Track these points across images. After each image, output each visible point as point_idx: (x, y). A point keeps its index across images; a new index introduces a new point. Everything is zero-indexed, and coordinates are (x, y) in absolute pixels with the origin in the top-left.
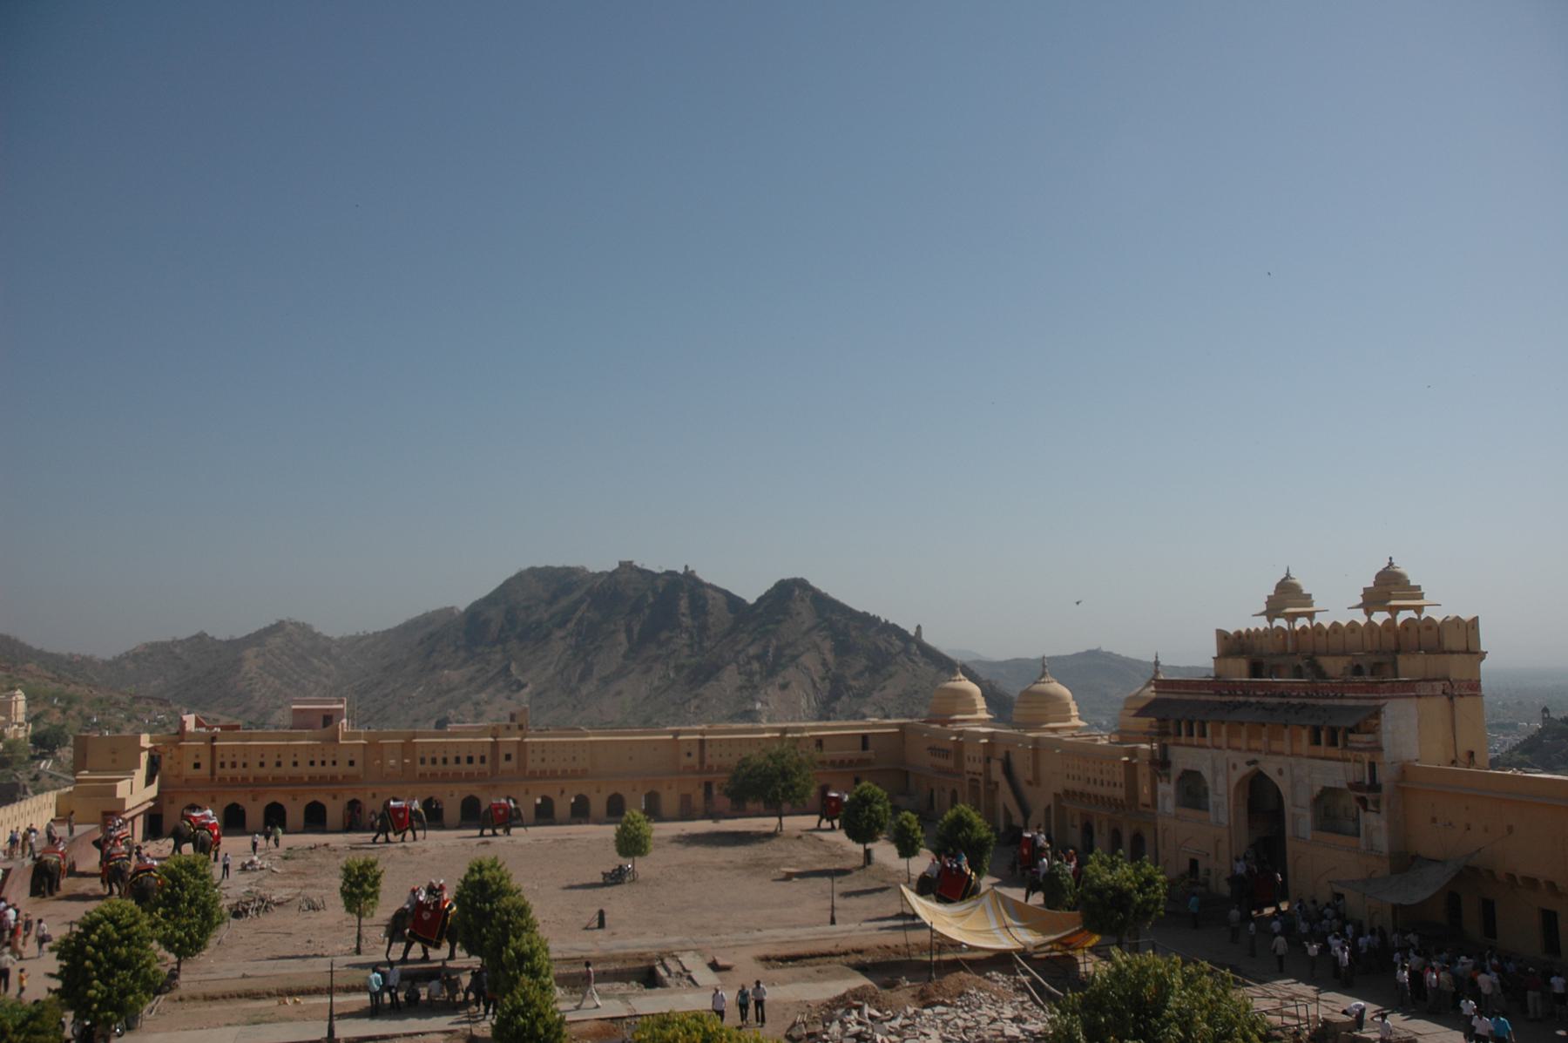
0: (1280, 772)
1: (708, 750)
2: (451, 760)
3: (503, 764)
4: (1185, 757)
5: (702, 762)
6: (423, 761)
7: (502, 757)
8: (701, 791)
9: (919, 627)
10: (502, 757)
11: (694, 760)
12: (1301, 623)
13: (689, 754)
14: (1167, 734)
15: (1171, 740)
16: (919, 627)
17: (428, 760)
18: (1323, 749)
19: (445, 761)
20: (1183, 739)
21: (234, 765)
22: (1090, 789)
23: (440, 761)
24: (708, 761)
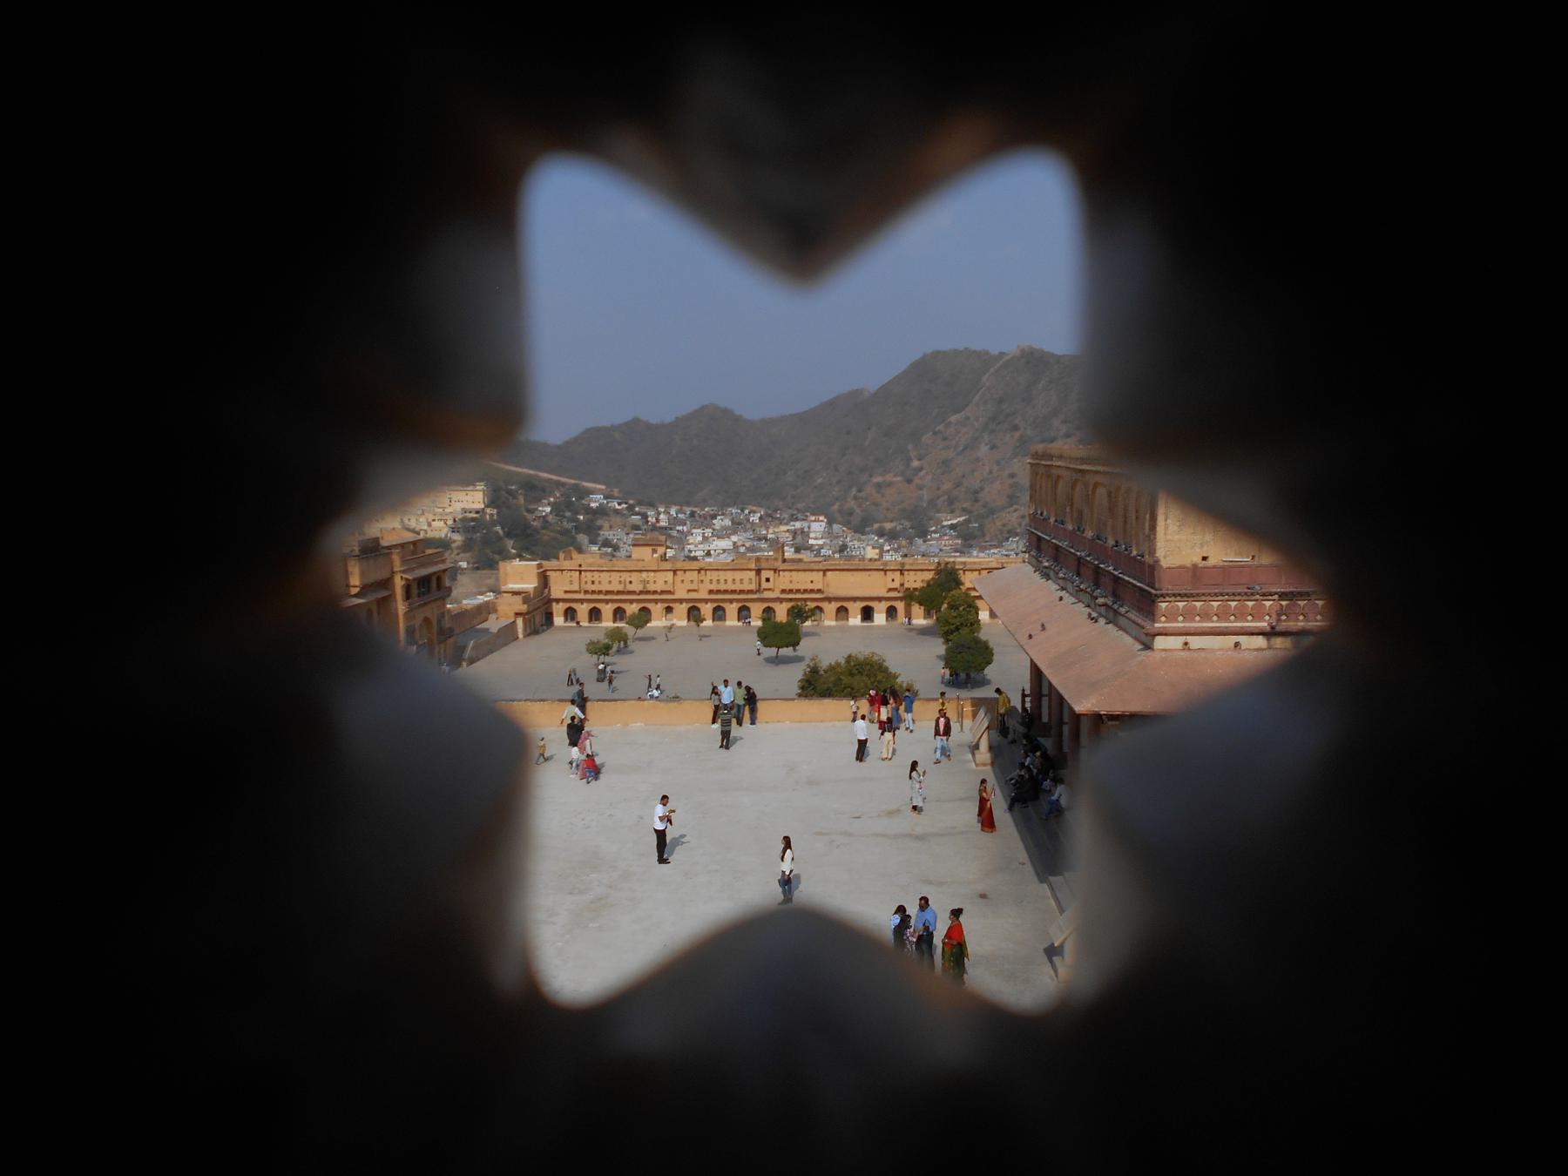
3: (765, 585)
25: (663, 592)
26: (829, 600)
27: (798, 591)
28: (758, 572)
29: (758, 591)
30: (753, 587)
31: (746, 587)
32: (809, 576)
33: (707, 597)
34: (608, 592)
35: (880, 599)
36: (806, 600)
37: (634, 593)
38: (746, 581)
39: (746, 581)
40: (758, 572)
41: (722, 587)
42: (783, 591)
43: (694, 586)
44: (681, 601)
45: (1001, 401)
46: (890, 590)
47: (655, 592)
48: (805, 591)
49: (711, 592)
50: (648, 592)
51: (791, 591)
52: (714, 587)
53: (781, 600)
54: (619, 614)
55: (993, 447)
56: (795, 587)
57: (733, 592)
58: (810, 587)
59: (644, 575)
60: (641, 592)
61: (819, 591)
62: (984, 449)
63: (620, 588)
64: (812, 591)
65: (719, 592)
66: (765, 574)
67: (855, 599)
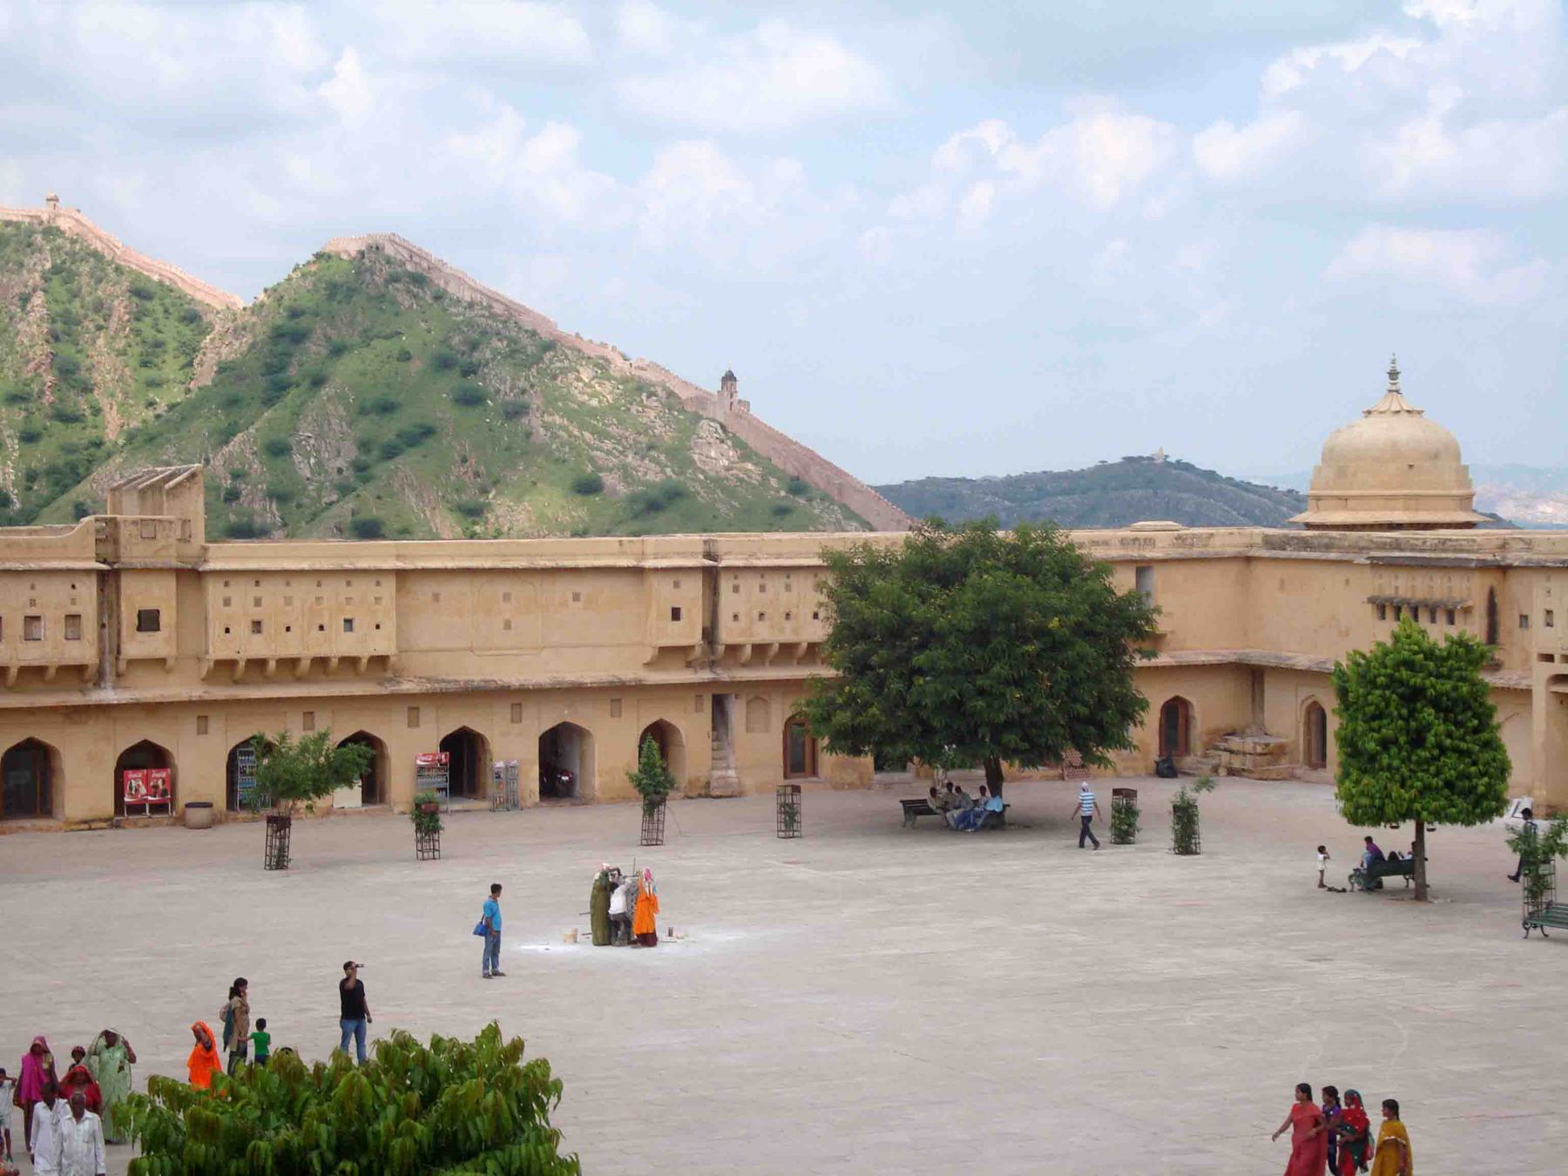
1: (729, 601)
5: (710, 634)
7: (129, 618)
8: (705, 718)
9: (729, 378)
10: (129, 618)
11: (688, 633)
13: (676, 614)
16: (729, 378)
24: (728, 633)
26: (413, 704)
28: (108, 579)
29: (99, 679)
30: (83, 652)
31: (53, 649)
35: (616, 693)
36: (309, 706)
38: (52, 629)
39: (52, 629)
40: (108, 579)
42: (225, 667)
48: (321, 663)
53: (202, 710)
58: (340, 645)
66: (136, 595)
67: (515, 697)
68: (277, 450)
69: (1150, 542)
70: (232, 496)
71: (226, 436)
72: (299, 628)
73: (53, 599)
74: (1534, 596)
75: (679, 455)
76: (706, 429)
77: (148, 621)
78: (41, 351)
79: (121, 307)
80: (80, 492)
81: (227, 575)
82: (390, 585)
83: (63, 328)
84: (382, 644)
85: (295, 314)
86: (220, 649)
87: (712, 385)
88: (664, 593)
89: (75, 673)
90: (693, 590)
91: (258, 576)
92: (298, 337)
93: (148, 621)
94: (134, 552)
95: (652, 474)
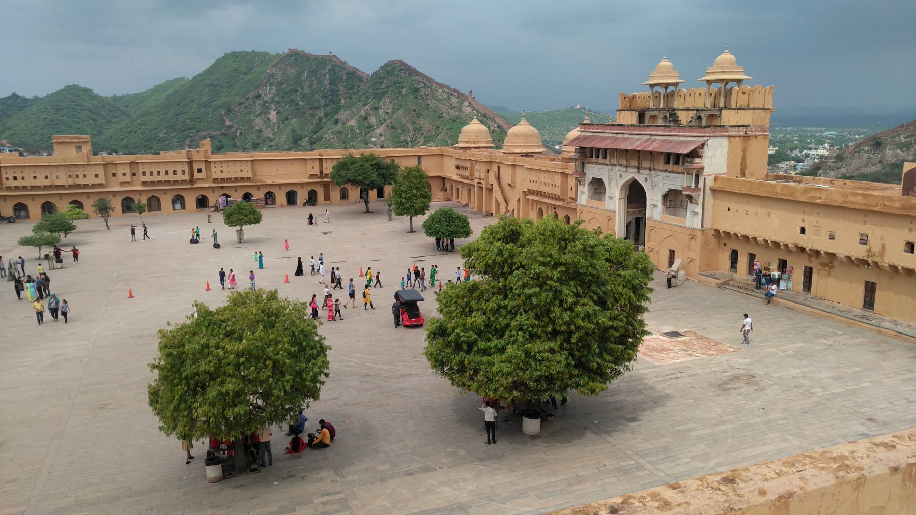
0: (646, 180)
2: (163, 173)
3: (197, 175)
4: (593, 171)
5: (321, 172)
6: (144, 174)
7: (196, 171)
11: (317, 171)
12: (670, 89)
14: (586, 156)
15: (588, 160)
17: (148, 174)
18: (670, 167)
19: (159, 173)
20: (594, 160)
21: (15, 179)
22: (543, 189)
23: (155, 174)
25: (94, 186)
26: (258, 187)
27: (229, 180)
28: (191, 163)
30: (186, 177)
31: (180, 177)
32: (238, 167)
33: (142, 188)
34: (33, 188)
35: (302, 184)
37: (63, 187)
39: (179, 172)
40: (191, 163)
41: (155, 178)
42: (215, 180)
43: (128, 178)
44: (114, 193)
45: (282, 84)
46: (311, 176)
47: (86, 186)
48: (236, 179)
49: (145, 183)
50: (78, 186)
51: (222, 180)
52: (148, 178)
54: (48, 208)
55: (279, 113)
56: (225, 175)
57: (168, 182)
58: (239, 175)
59: (74, 169)
60: (71, 187)
61: (249, 179)
62: (273, 115)
63: (47, 183)
64: (242, 179)
65: (153, 183)
66: (196, 167)
67: (281, 185)
68: (376, 109)
69: (420, 151)
70: (366, 119)
71: (365, 105)
72: (231, 172)
73: (179, 169)
74: (477, 167)
75: (460, 110)
76: (466, 103)
77: (200, 171)
78: (328, 87)
79: (344, 77)
80: (336, 117)
81: (215, 162)
82: (250, 163)
83: (332, 82)
84: (250, 175)
85: (380, 78)
86: (214, 176)
87: (467, 94)
88: (310, 164)
89: (184, 182)
90: (317, 165)
91: (221, 162)
92: (381, 83)
93: (200, 171)
94: (196, 157)
95: (454, 113)
